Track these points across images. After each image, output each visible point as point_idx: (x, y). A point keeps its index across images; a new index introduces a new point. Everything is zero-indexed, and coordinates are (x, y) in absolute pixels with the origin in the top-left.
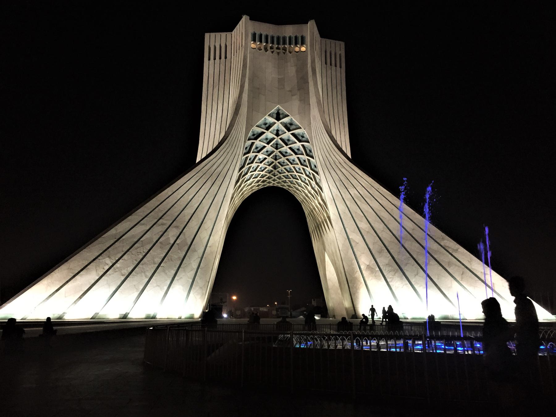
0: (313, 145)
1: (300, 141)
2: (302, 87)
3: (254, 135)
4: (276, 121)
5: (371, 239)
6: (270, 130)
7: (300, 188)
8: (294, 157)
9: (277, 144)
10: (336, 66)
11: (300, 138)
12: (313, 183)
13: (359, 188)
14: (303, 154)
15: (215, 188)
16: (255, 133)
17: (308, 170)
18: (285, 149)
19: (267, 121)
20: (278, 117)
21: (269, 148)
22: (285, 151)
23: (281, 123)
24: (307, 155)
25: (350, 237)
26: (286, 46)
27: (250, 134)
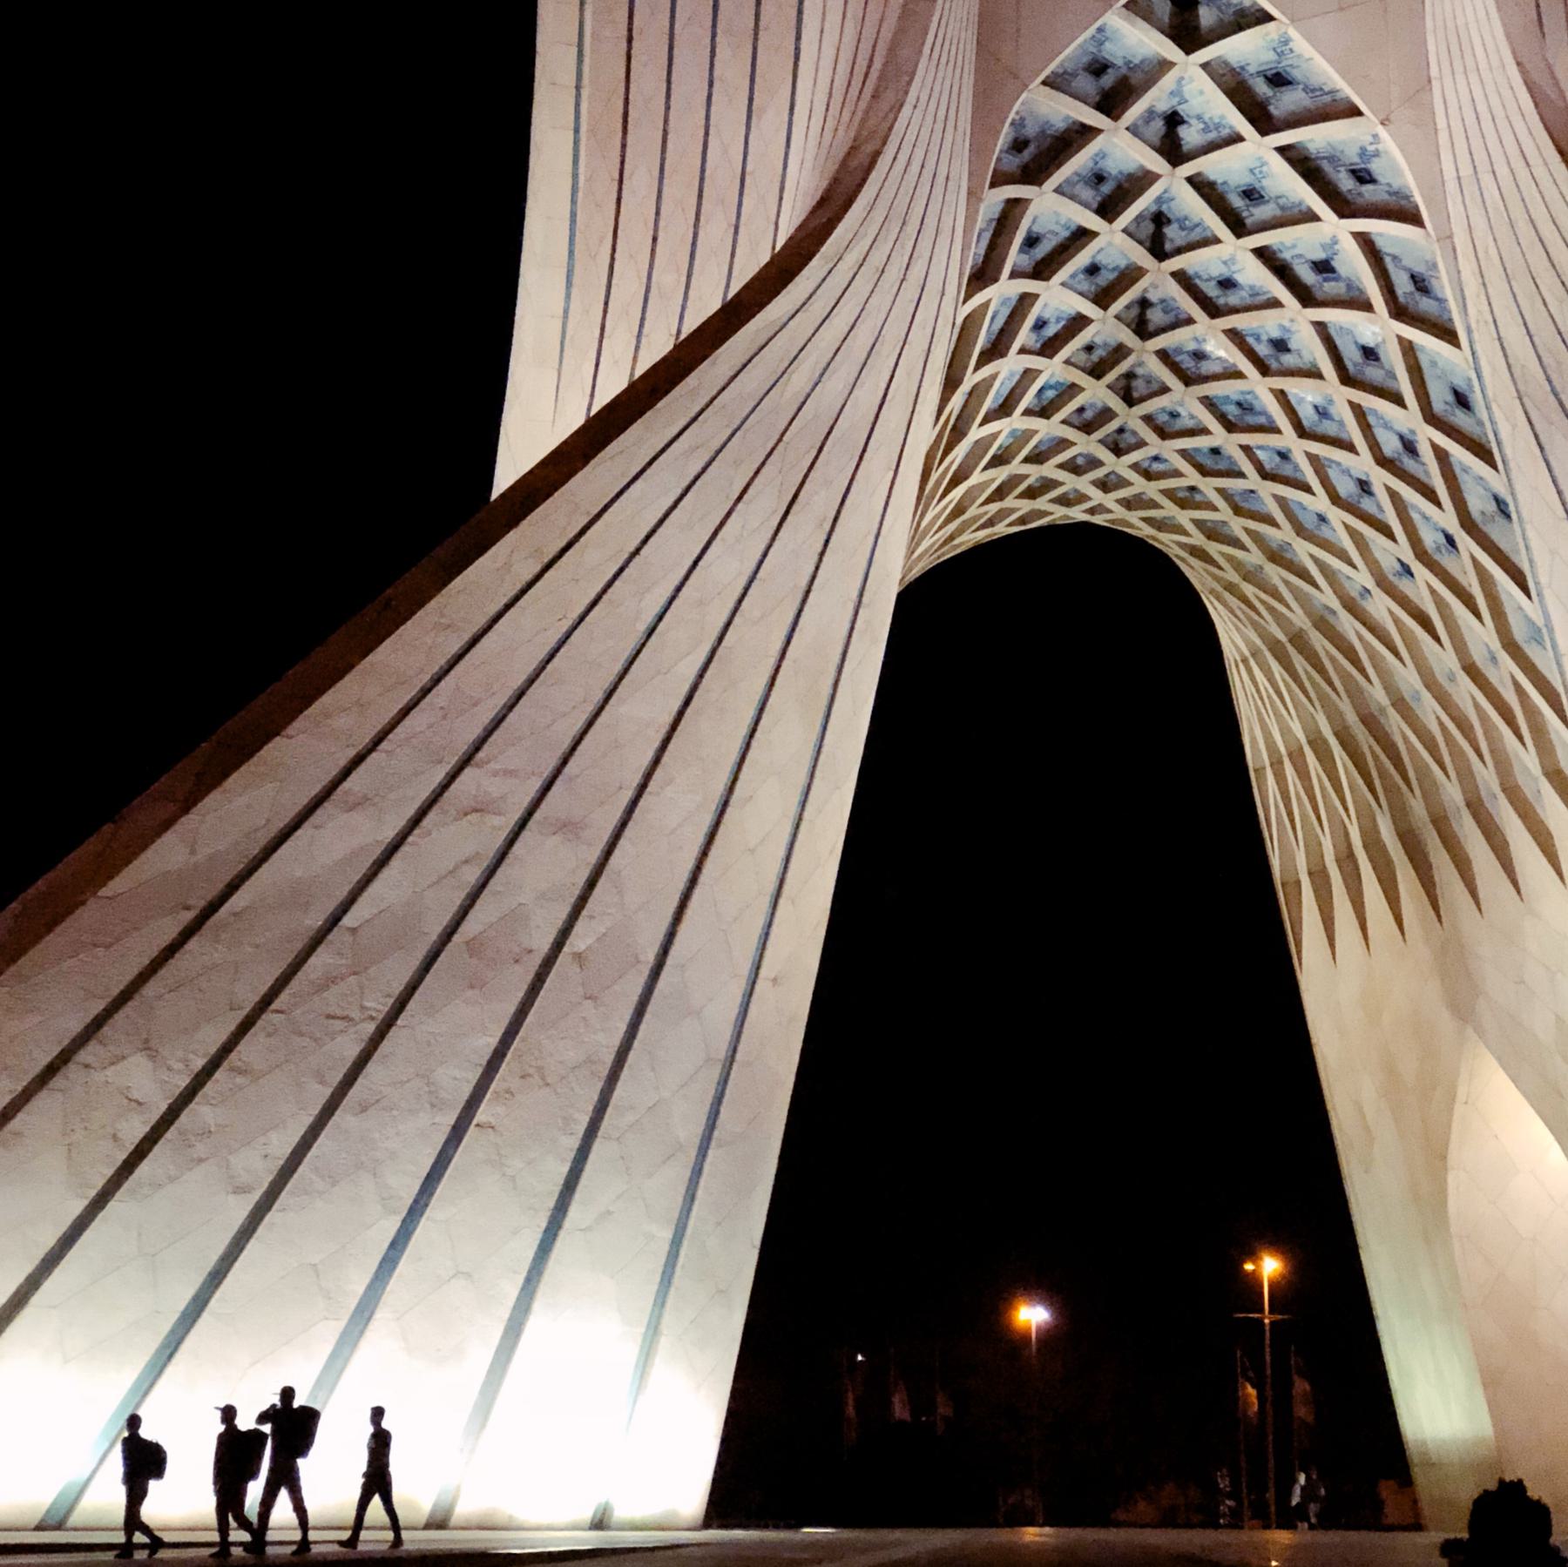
0: (1447, 238)
1: (1344, 207)
3: (1018, 145)
7: (1303, 551)
8: (1295, 321)
9: (1159, 219)
11: (1346, 183)
14: (1363, 304)
16: (1031, 130)
18: (1230, 257)
21: (1114, 244)
22: (1218, 271)
23: (1205, 66)
24: (1399, 312)
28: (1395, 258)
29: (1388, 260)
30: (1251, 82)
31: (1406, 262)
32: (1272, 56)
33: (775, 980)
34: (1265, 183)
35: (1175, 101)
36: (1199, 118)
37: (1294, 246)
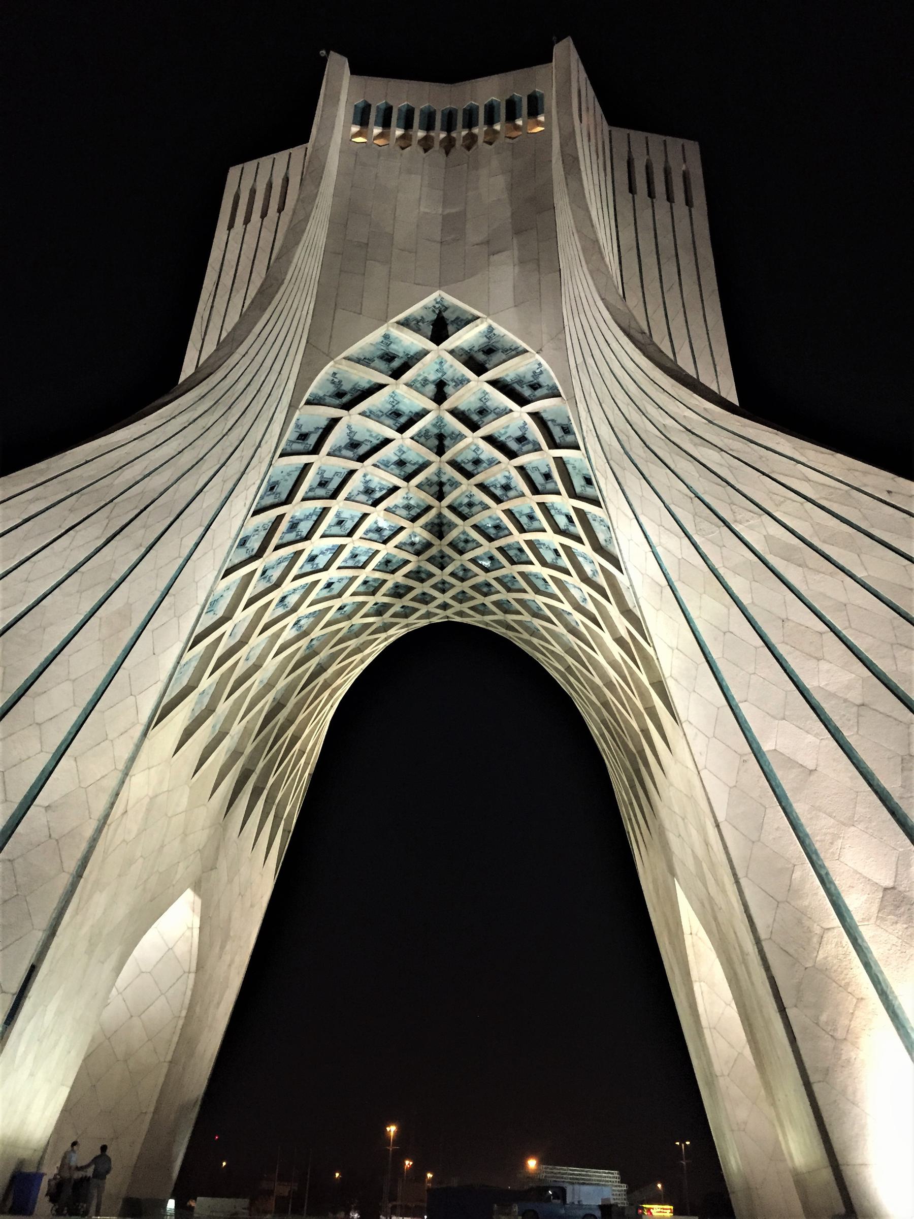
2: (531, 225)
3: (340, 395)
4: (430, 345)
6: (408, 376)
12: (584, 550)
14: (537, 448)
15: (122, 553)
16: (346, 387)
17: (563, 503)
18: (471, 443)
19: (394, 348)
20: (439, 330)
21: (404, 444)
22: (471, 456)
25: (766, 746)
27: (318, 384)
28: (553, 421)
29: (550, 424)
30: (475, 355)
31: (559, 421)
32: (485, 340)
33: (47, 808)
34: (488, 404)
35: (440, 375)
36: (453, 380)
37: (506, 432)
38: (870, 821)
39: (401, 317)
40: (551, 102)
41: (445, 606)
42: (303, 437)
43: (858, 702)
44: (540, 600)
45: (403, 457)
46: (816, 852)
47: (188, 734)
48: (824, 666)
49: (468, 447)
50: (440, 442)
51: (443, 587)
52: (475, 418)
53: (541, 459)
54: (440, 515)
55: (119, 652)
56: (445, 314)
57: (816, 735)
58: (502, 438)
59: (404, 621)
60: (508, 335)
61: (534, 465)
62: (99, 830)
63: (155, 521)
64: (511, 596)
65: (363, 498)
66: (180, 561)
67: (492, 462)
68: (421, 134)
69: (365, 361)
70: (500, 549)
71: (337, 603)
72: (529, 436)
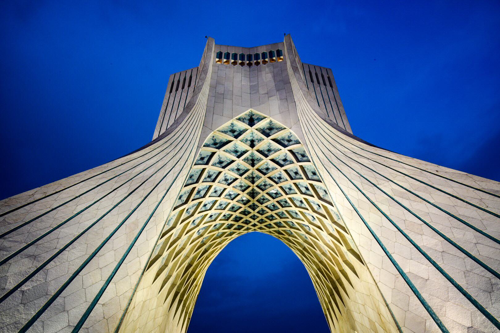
4: (249, 127)
5: (456, 265)
6: (241, 138)
10: (325, 84)
13: (400, 179)
14: (292, 162)
15: (135, 199)
16: (218, 141)
17: (304, 182)
18: (265, 162)
19: (235, 128)
20: (251, 121)
21: (240, 162)
22: (265, 167)
25: (406, 271)
26: (259, 61)
27: (208, 140)
33: (103, 305)
38: (456, 299)
39: (238, 117)
40: (285, 51)
41: (254, 225)
42: (202, 159)
43: (441, 251)
44: (294, 221)
45: (239, 167)
46: (434, 314)
47: (158, 275)
48: (424, 237)
49: (264, 163)
50: (253, 162)
51: (254, 218)
52: (266, 153)
53: (295, 166)
54: (253, 190)
55: (133, 239)
56: (253, 117)
57: (426, 265)
58: (277, 160)
59: (238, 231)
60: (277, 122)
61: (291, 169)
62: (124, 315)
63: (148, 187)
64: (282, 221)
65: (224, 182)
66: (157, 203)
67: (273, 169)
68: (240, 61)
69: (225, 132)
70: (277, 202)
71: (214, 223)
72: (288, 159)
